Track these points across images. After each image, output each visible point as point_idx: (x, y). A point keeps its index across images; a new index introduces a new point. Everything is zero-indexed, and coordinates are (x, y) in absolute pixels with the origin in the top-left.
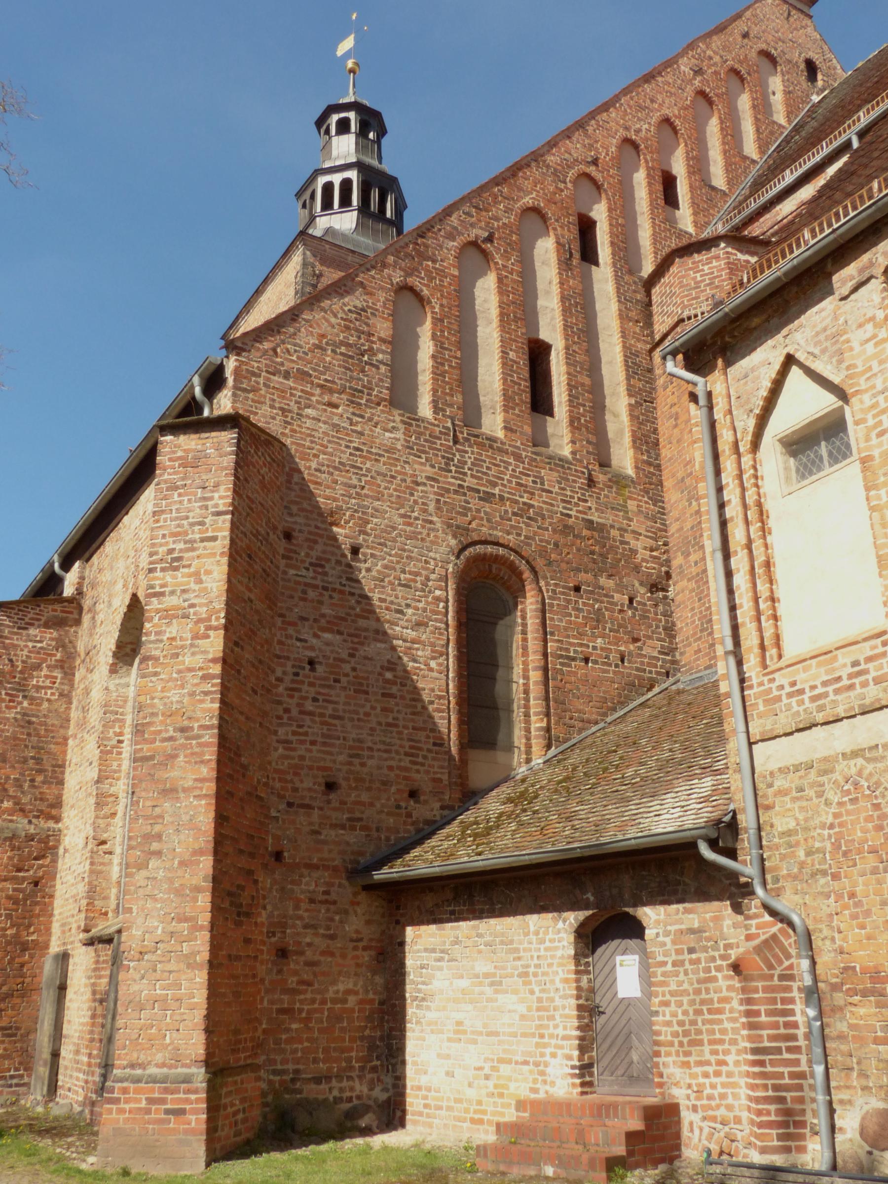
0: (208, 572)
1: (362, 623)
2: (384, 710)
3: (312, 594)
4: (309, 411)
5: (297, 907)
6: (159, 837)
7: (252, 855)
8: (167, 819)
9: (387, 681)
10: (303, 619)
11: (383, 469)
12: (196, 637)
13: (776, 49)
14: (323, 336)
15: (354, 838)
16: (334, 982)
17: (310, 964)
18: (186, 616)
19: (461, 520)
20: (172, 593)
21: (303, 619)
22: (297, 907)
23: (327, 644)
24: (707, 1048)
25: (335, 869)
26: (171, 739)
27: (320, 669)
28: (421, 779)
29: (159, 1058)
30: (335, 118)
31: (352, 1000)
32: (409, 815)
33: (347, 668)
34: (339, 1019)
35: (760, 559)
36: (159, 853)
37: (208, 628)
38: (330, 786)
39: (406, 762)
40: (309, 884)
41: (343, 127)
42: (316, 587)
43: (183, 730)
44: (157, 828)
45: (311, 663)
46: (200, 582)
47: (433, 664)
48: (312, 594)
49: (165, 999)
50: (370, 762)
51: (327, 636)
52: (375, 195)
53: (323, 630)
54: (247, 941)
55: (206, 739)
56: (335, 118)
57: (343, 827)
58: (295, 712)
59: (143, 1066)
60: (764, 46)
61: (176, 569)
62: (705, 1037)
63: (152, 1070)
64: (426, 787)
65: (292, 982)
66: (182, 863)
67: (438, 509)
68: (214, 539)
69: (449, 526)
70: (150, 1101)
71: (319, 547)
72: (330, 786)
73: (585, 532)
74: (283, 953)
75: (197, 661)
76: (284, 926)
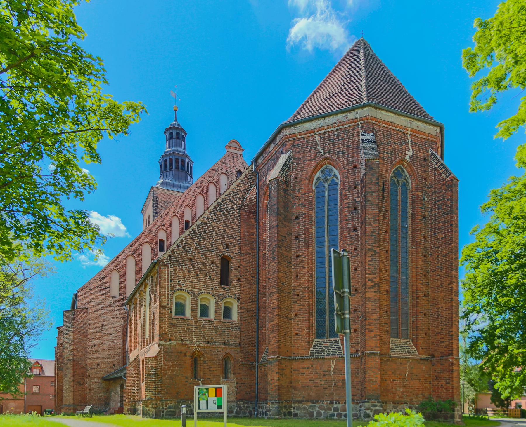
15: (102, 373)
25: (99, 378)
27: (96, 347)
28: (115, 362)
38: (98, 365)
40: (95, 380)
45: (94, 345)
54: (82, 388)
60: (223, 171)
64: (116, 364)
65: (92, 394)
75: (70, 349)
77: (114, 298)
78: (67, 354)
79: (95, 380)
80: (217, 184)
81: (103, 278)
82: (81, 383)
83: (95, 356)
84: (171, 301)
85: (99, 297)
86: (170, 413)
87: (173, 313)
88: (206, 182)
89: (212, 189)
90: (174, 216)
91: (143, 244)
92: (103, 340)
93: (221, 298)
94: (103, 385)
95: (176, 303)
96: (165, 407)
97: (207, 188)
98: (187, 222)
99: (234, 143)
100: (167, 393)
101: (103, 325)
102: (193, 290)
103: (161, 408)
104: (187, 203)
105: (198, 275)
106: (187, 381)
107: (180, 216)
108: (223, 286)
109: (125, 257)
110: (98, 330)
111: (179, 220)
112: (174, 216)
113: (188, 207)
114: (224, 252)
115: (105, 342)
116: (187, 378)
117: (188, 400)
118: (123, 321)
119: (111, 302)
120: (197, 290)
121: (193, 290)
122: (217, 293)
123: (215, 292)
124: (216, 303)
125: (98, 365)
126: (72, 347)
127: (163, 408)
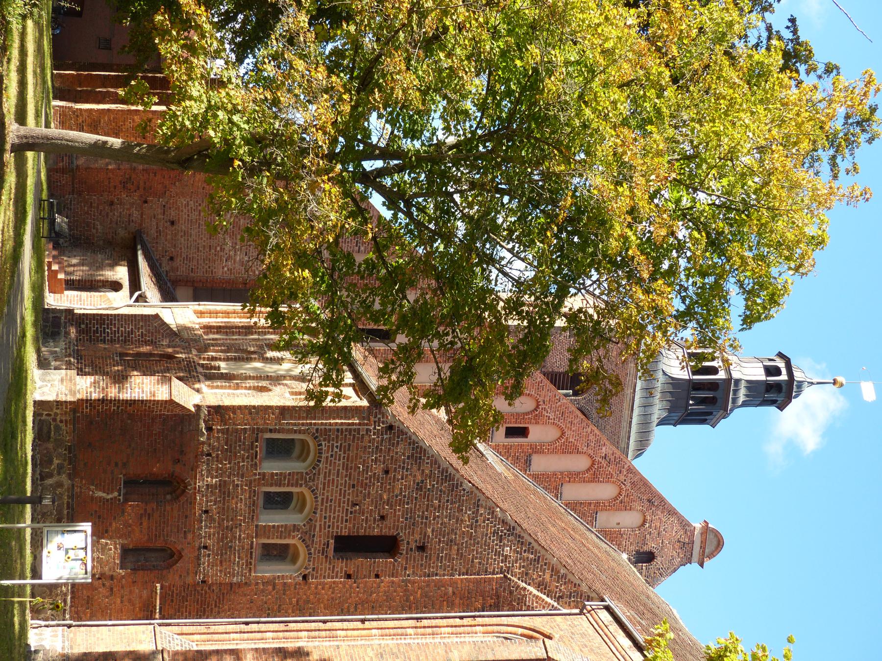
5: (128, 209)
7: (144, 189)
13: (650, 527)
15: (153, 232)
16: (101, 224)
22: (128, 209)
25: (141, 225)
28: (178, 262)
30: (781, 364)
32: (163, 256)
34: (88, 226)
38: (173, 223)
39: (184, 256)
41: (772, 371)
47: (226, 269)
52: (709, 395)
54: (115, 187)
56: (781, 364)
58: (200, 208)
65: (101, 207)
76: (120, 204)
79: (136, 214)
80: (619, 504)
82: (129, 185)
83: (194, 216)
84: (295, 431)
86: (45, 430)
87: (268, 436)
88: (622, 478)
89: (604, 491)
90: (538, 402)
93: (307, 538)
94: (122, 233)
95: (293, 439)
96: (58, 419)
97: (608, 479)
98: (523, 432)
99: (715, 543)
100: (91, 423)
102: (322, 476)
103: (58, 411)
104: (568, 433)
105: (353, 486)
106: (116, 464)
107: (536, 415)
108: (332, 541)
111: (527, 414)
112: (538, 402)
113: (558, 434)
114: (408, 543)
115: (228, 240)
116: (124, 465)
117: (74, 468)
120: (321, 486)
121: (322, 476)
122: (317, 529)
123: (318, 524)
124: (295, 528)
125: (173, 223)
127: (56, 414)
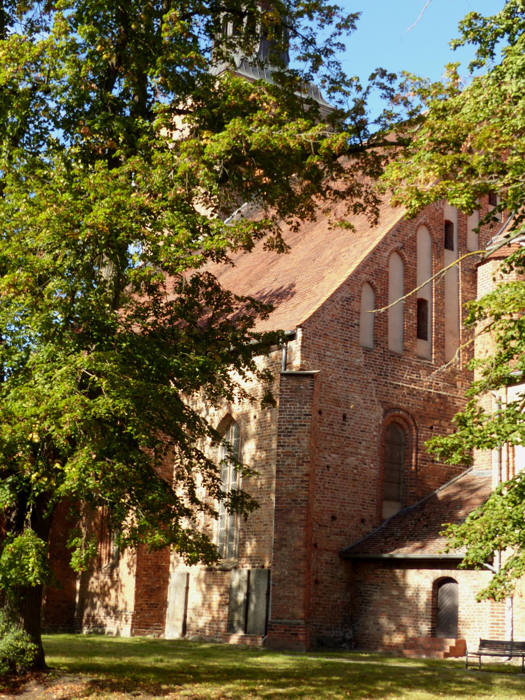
0: (303, 439)
1: (346, 449)
2: (354, 486)
3: (328, 438)
4: (328, 353)
6: (285, 540)
8: (289, 533)
9: (355, 474)
10: (325, 449)
11: (355, 377)
12: (298, 465)
14: (334, 315)
15: (341, 539)
17: (326, 587)
18: (294, 456)
19: (385, 399)
20: (288, 446)
21: (325, 449)
23: (334, 459)
24: (476, 623)
25: (334, 552)
26: (289, 504)
27: (331, 470)
28: (366, 515)
29: (287, 616)
31: (339, 601)
33: (340, 469)
35: (511, 466)
36: (285, 546)
37: (303, 462)
42: (329, 434)
43: (294, 500)
44: (285, 536)
45: (328, 467)
46: (299, 442)
47: (372, 465)
48: (328, 438)
49: (289, 597)
50: (348, 508)
51: (334, 455)
53: (333, 453)
55: (303, 505)
57: (337, 534)
58: (322, 488)
59: (281, 619)
61: (289, 436)
62: (476, 620)
63: (285, 620)
65: (320, 593)
66: (295, 550)
67: (377, 394)
68: (305, 425)
69: (380, 401)
70: (285, 630)
71: (331, 417)
72: (334, 518)
73: (437, 400)
74: (316, 582)
76: (317, 572)
77: (367, 351)
78: (290, 487)
81: (348, 300)
85: (339, 345)
91: (418, 226)
92: (345, 456)
94: (340, 572)
101: (344, 417)
109: (386, 254)
110: (336, 427)
118: (382, 410)
119: (360, 361)
125: (334, 518)
126: (305, 468)
